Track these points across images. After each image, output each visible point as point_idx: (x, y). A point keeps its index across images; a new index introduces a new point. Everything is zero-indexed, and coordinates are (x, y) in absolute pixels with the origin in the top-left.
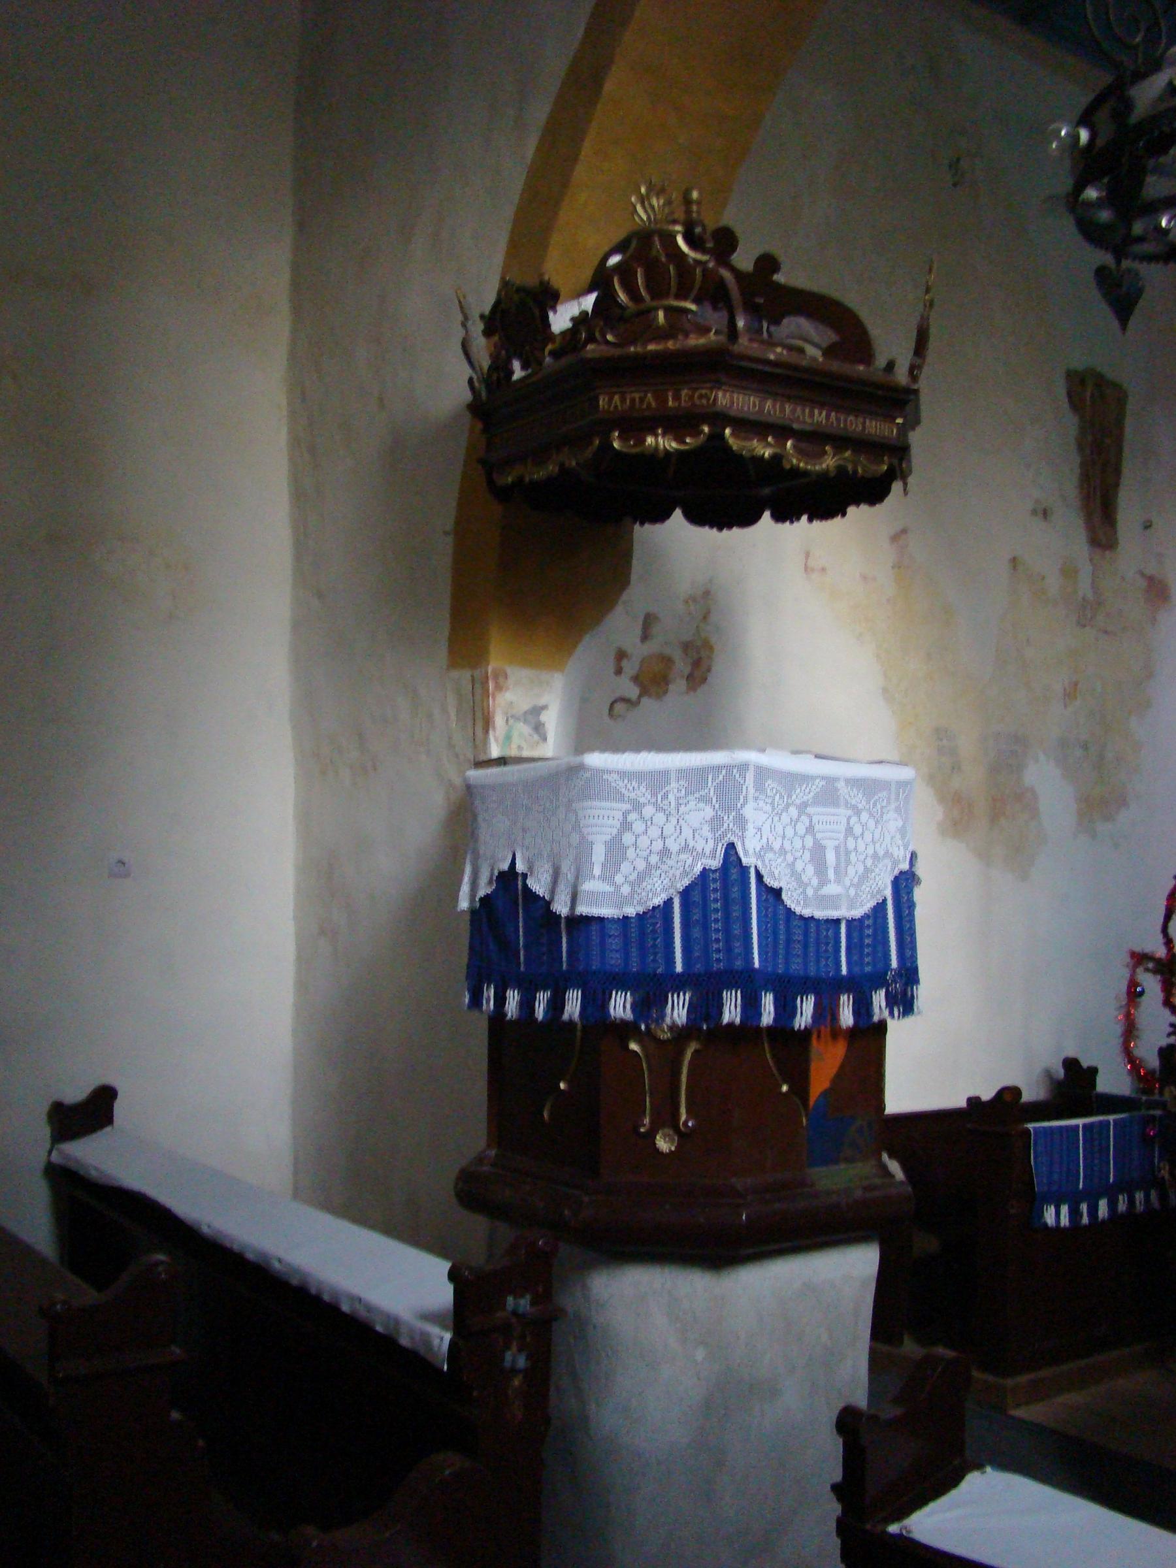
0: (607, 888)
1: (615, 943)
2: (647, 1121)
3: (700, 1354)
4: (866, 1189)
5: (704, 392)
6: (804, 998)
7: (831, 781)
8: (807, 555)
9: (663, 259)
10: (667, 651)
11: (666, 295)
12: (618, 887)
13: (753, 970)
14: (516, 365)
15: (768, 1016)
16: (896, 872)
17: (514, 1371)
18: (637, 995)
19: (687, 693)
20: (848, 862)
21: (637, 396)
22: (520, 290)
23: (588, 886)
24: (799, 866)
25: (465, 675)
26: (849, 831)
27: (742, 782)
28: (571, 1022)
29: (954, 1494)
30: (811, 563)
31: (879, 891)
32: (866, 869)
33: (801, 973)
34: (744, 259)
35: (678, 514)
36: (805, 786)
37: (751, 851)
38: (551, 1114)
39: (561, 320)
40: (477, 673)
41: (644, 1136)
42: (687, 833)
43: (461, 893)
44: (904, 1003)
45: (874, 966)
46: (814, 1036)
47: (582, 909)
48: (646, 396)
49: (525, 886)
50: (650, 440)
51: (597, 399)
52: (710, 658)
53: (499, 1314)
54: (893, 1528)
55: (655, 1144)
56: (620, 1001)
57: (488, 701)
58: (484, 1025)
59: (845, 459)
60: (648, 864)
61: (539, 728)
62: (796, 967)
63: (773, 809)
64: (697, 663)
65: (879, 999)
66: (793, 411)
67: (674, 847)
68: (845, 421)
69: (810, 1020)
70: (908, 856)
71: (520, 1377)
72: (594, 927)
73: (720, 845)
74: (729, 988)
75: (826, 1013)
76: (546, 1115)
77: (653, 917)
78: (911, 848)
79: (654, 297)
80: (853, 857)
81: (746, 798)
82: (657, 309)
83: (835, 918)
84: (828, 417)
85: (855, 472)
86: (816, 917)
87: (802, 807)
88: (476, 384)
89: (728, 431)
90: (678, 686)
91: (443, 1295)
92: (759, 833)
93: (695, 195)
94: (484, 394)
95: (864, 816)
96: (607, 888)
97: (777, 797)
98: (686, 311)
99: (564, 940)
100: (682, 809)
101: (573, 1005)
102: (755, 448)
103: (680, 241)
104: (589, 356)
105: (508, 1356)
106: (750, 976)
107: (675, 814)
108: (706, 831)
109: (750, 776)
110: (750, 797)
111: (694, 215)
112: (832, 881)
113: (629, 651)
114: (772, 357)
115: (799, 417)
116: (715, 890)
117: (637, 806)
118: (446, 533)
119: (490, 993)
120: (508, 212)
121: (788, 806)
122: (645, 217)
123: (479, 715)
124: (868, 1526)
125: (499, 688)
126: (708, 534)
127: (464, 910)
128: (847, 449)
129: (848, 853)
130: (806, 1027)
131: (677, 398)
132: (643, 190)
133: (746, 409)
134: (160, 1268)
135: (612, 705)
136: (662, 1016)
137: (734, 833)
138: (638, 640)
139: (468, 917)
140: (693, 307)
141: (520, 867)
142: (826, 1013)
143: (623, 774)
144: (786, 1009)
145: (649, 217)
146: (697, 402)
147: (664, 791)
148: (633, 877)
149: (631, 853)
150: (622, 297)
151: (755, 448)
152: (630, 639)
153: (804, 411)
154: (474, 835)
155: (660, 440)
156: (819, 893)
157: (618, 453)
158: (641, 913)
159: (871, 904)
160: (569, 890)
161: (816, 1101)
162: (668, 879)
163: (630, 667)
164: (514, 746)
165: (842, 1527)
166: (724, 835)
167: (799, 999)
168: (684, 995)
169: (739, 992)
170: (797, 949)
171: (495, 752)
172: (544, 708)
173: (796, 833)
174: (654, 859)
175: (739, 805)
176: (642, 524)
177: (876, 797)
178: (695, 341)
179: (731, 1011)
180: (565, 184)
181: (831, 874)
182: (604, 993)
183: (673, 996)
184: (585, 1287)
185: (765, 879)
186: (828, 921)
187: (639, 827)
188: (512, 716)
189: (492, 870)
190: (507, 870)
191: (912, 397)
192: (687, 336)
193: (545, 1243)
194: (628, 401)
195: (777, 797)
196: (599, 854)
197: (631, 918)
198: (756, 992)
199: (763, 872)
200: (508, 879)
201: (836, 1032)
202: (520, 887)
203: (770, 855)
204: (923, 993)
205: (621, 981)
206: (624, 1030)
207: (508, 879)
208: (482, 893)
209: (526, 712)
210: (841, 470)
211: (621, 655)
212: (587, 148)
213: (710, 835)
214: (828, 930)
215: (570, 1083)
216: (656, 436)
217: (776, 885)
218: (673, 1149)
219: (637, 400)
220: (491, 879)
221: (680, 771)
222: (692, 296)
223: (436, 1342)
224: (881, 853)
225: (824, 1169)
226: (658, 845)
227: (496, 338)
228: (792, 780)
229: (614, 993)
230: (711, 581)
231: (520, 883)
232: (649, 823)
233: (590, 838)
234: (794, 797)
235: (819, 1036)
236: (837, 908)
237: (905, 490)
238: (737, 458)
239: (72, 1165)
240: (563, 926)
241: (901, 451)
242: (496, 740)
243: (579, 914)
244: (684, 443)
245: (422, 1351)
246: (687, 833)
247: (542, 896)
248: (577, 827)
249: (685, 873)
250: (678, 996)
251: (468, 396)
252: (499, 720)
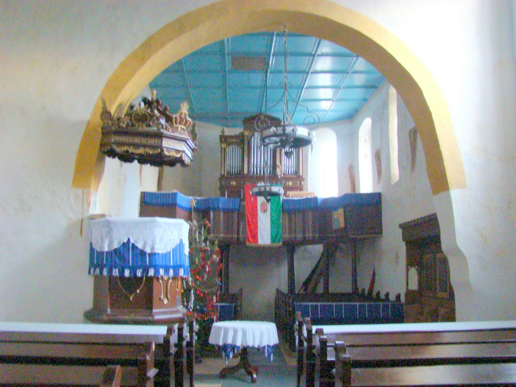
25: (80, 191)
38: (133, 298)
40: (85, 191)
76: (131, 299)
141: (132, 241)
196: (158, 240)
205: (162, 267)
215: (140, 291)
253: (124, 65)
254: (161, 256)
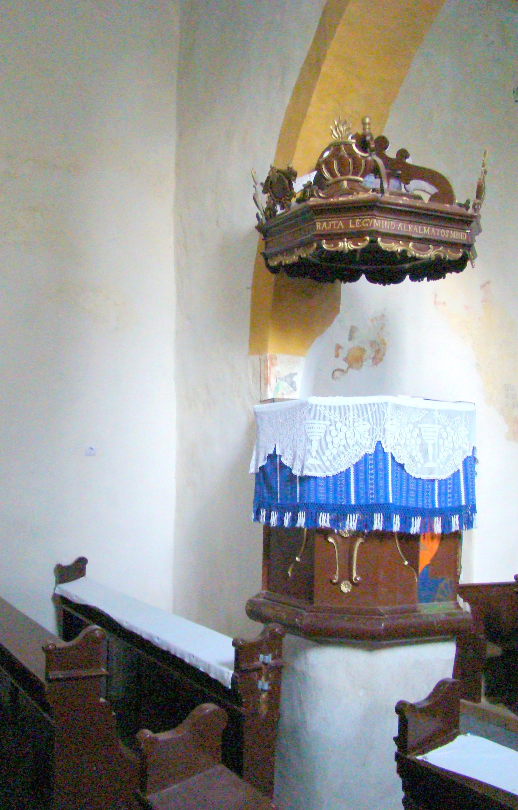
0: (317, 462)
1: (322, 490)
2: (337, 577)
3: (361, 693)
4: (446, 614)
5: (367, 220)
6: (416, 518)
7: (431, 411)
8: (436, 296)
9: (346, 156)
10: (362, 346)
11: (348, 174)
12: (323, 462)
13: (389, 504)
14: (278, 207)
15: (396, 527)
16: (465, 457)
17: (263, 690)
18: (332, 515)
19: (373, 366)
20: (439, 452)
21: (334, 222)
22: (278, 171)
23: (310, 461)
24: (414, 453)
25: (256, 358)
26: (440, 436)
27: (385, 411)
28: (300, 529)
29: (451, 744)
30: (437, 300)
31: (455, 466)
32: (449, 455)
33: (414, 506)
34: (391, 153)
35: (363, 277)
36: (417, 414)
37: (389, 446)
38: (292, 573)
39: (298, 186)
40: (262, 357)
41: (335, 584)
42: (358, 436)
43: (251, 465)
44: (469, 523)
45: (453, 503)
46: (422, 537)
47: (306, 473)
48: (339, 222)
49: (280, 461)
50: (341, 244)
51: (315, 224)
52: (385, 349)
53: (256, 663)
54: (419, 757)
55: (341, 588)
56: (324, 517)
57: (267, 371)
58: (261, 530)
59: (440, 251)
60: (338, 451)
61: (292, 384)
62: (412, 503)
63: (401, 424)
64: (378, 351)
65: (455, 520)
66: (413, 229)
67: (351, 442)
68: (440, 233)
69: (418, 530)
70: (472, 449)
71: (266, 693)
72: (312, 481)
73: (374, 442)
74: (377, 513)
75: (427, 526)
76: (289, 573)
77: (340, 477)
78: (473, 445)
79: (342, 174)
80: (442, 449)
81: (387, 420)
82: (343, 180)
83: (432, 479)
84: (431, 230)
85: (445, 258)
86: (422, 478)
87: (415, 425)
88: (261, 217)
89: (379, 239)
91: (230, 654)
92: (393, 436)
93: (367, 120)
94: (264, 221)
95: (448, 429)
96: (317, 462)
97: (403, 419)
98: (357, 181)
99: (298, 488)
100: (355, 424)
101: (302, 520)
102: (393, 247)
103: (354, 146)
104: (311, 203)
105: (260, 683)
106: (387, 507)
107: (352, 427)
108: (367, 435)
109: (389, 409)
110: (389, 419)
111: (367, 130)
112: (431, 461)
113: (342, 345)
114: (401, 202)
115: (415, 230)
116: (371, 464)
117: (334, 423)
118: (248, 288)
119: (263, 513)
120: (277, 131)
121: (408, 423)
122: (337, 136)
123: (263, 378)
124: (408, 756)
125: (273, 364)
126: (378, 287)
127: (252, 473)
128: (440, 246)
129: (439, 446)
130: (416, 533)
131: (354, 223)
132: (336, 123)
133: (388, 228)
134: (97, 632)
135: (333, 373)
136: (344, 526)
137: (381, 437)
138: (347, 341)
139: (254, 477)
140: (361, 179)
141: (278, 452)
142: (427, 526)
143: (327, 407)
144: (406, 522)
145: (339, 136)
146: (363, 225)
147: (347, 415)
148: (331, 458)
149: (330, 446)
150: (327, 175)
151: (393, 247)
152: (344, 341)
153: (418, 228)
154: (257, 438)
155: (346, 243)
156: (424, 466)
157: (325, 250)
158: (335, 475)
159: (452, 472)
160: (300, 463)
161: (424, 569)
162: (348, 459)
163: (343, 354)
164: (280, 393)
165: (398, 757)
166: (376, 437)
167: (413, 518)
168: (355, 515)
169: (382, 514)
170: (412, 494)
171: (270, 396)
172: (296, 374)
173: (412, 437)
174: (341, 449)
175: (383, 423)
176: (345, 283)
177: (455, 419)
178: (362, 196)
179: (378, 524)
180: (304, 116)
181: (430, 457)
182: (316, 513)
183: (349, 516)
184: (306, 658)
185: (396, 459)
186: (428, 480)
187: (334, 433)
188: (279, 378)
189: (265, 453)
190: (272, 453)
191: (474, 219)
192: (358, 193)
193: (280, 630)
194: (330, 225)
195: (403, 419)
196: (315, 446)
197: (330, 477)
198: (390, 515)
199: (395, 456)
200: (272, 457)
201: (433, 537)
202: (278, 462)
203: (399, 447)
204: (478, 518)
205: (323, 508)
206: (325, 533)
207: (272, 457)
208: (261, 464)
209: (286, 377)
210: (438, 258)
211: (338, 347)
212: (315, 97)
213: (369, 437)
214: (428, 485)
215: (301, 558)
216: (344, 242)
217: (401, 462)
218: (349, 591)
219: (335, 225)
220: (265, 457)
221: (354, 406)
222: (359, 175)
223: (226, 675)
224: (457, 447)
225: (426, 604)
226: (343, 442)
227: (268, 194)
228: (410, 411)
229: (321, 513)
230: (385, 309)
231: (278, 460)
232: (339, 431)
233: (311, 438)
234: (411, 419)
235: (424, 538)
236: (433, 474)
237: (472, 265)
238: (383, 252)
239: (65, 595)
240: (298, 480)
241: (469, 246)
242: (271, 390)
243: (305, 475)
244: (358, 245)
245: (220, 680)
246: (358, 436)
247: (288, 466)
248: (304, 432)
249: (356, 456)
250: (352, 516)
251: (256, 223)
252: (272, 380)
253: (297, 93)
254: (321, 483)
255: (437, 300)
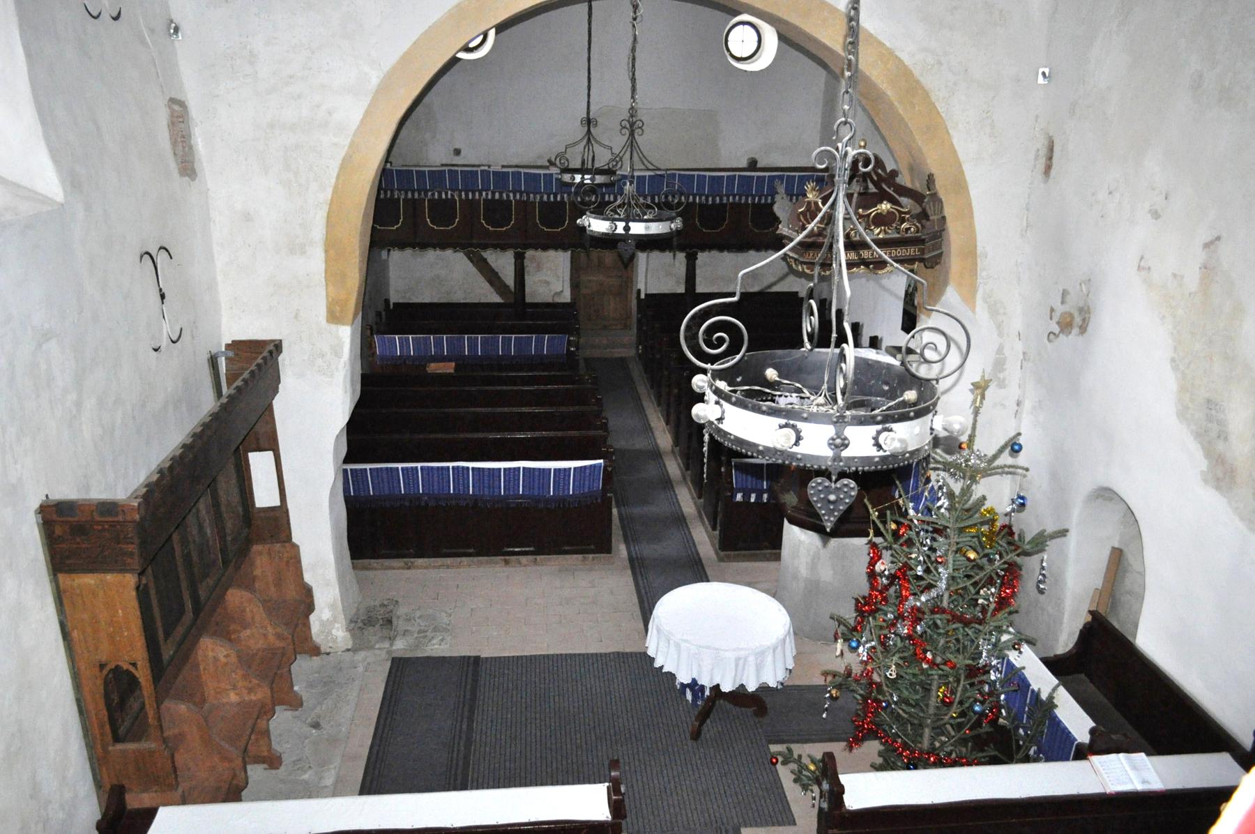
10: (1072, 311)
30: (1142, 264)
90: (1075, 331)
163: (1056, 316)
211: (1052, 310)
255: (1142, 264)
